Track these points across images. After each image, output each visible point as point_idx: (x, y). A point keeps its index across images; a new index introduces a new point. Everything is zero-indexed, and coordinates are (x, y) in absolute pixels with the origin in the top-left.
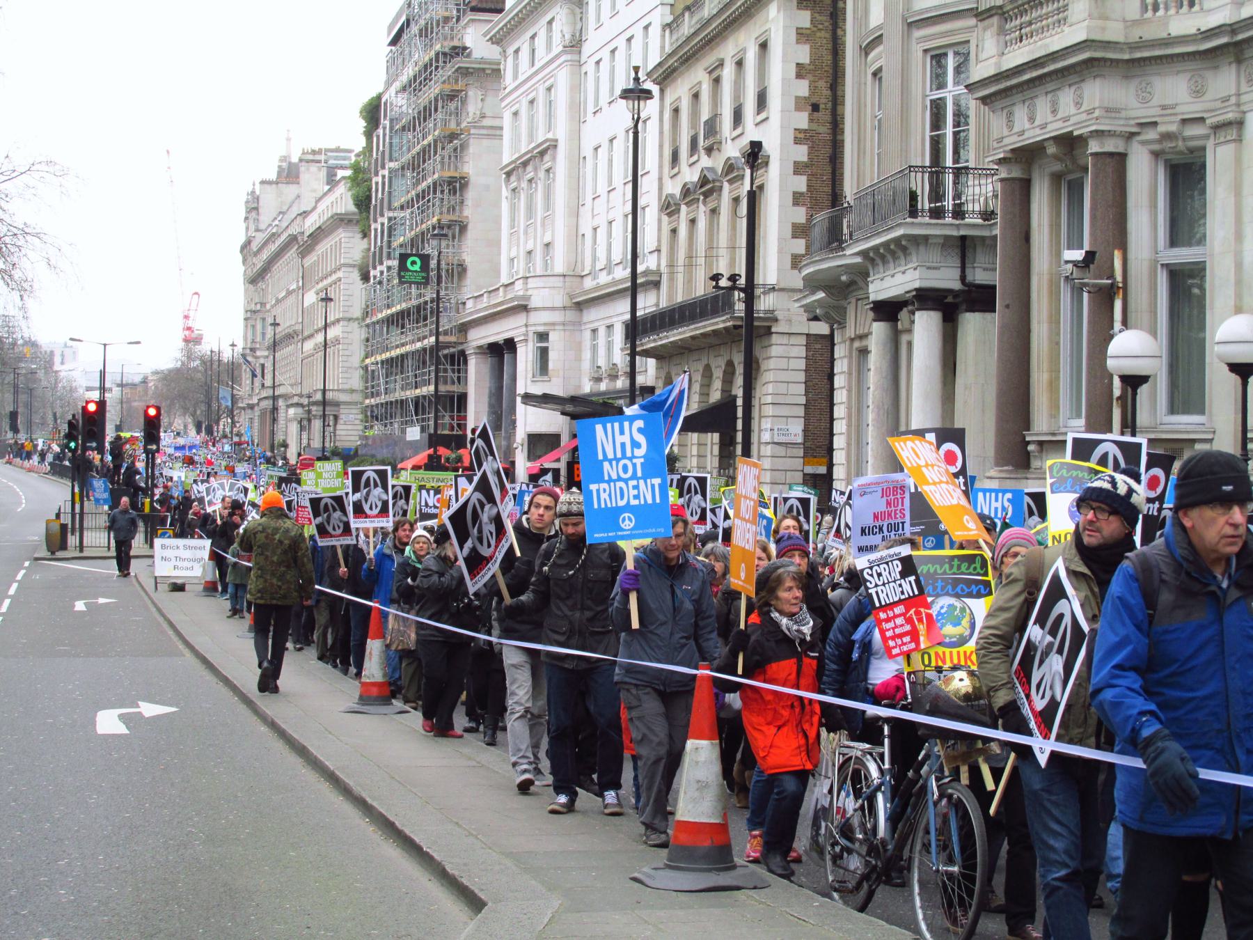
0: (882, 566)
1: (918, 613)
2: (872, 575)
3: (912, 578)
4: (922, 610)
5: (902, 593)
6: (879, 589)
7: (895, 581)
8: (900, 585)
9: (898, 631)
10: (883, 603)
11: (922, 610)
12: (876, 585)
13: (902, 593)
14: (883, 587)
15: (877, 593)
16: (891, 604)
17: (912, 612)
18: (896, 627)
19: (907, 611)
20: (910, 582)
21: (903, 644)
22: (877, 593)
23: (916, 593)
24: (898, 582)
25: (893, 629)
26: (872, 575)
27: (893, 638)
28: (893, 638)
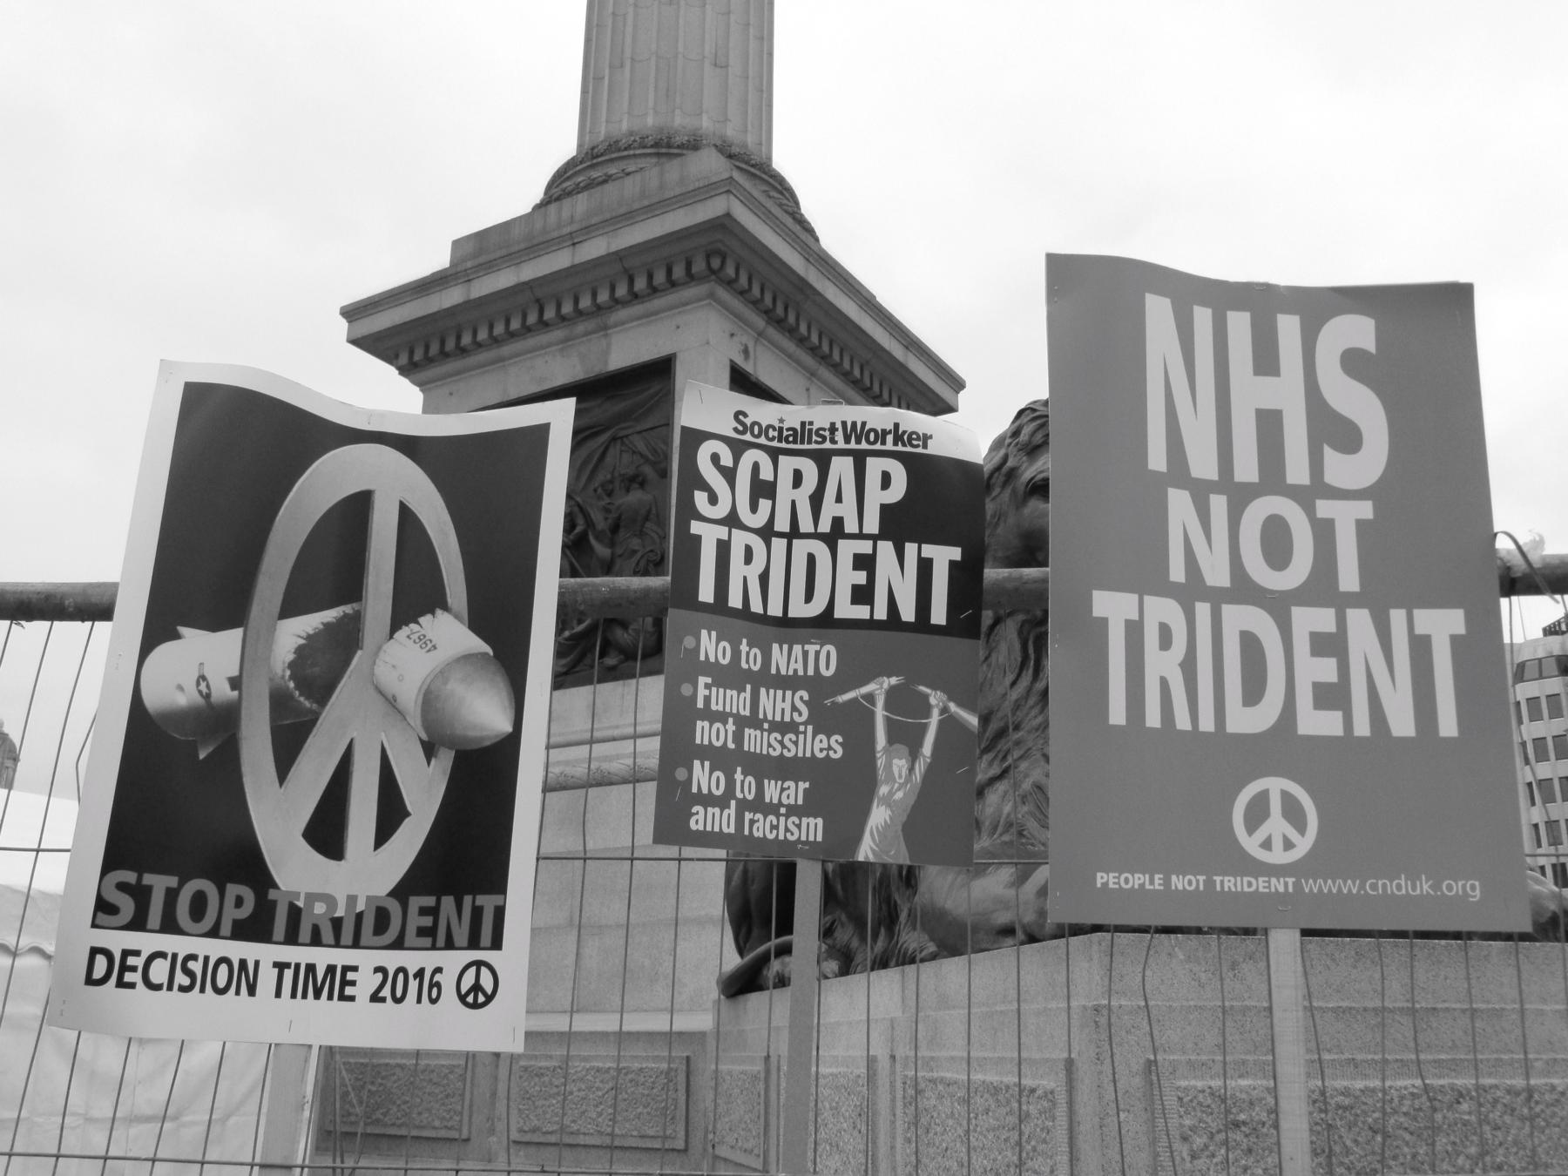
0: (787, 464)
1: (906, 704)
2: (730, 475)
3: (943, 556)
4: (936, 698)
5: (863, 595)
6: (740, 539)
7: (836, 533)
8: (865, 563)
9: (754, 741)
10: (735, 601)
11: (936, 698)
12: (732, 521)
13: (863, 595)
14: (758, 544)
15: (723, 548)
16: (764, 619)
17: (879, 687)
18: (754, 721)
19: (849, 675)
20: (925, 567)
21: (759, 805)
22: (723, 548)
23: (939, 615)
24: (865, 547)
25: (741, 723)
26: (730, 475)
27: (721, 759)
28: (721, 759)
